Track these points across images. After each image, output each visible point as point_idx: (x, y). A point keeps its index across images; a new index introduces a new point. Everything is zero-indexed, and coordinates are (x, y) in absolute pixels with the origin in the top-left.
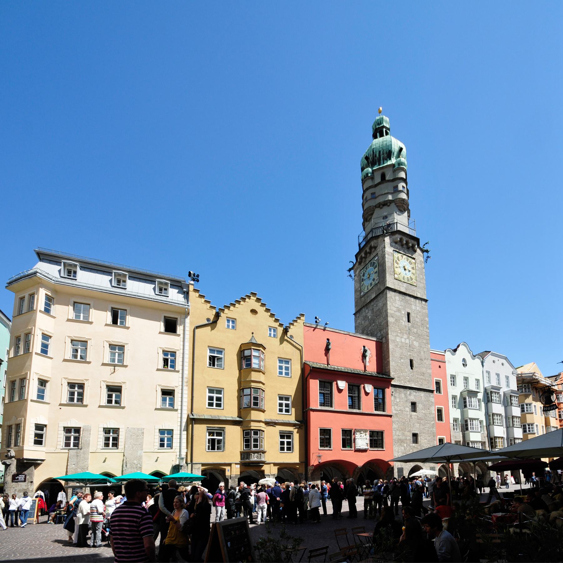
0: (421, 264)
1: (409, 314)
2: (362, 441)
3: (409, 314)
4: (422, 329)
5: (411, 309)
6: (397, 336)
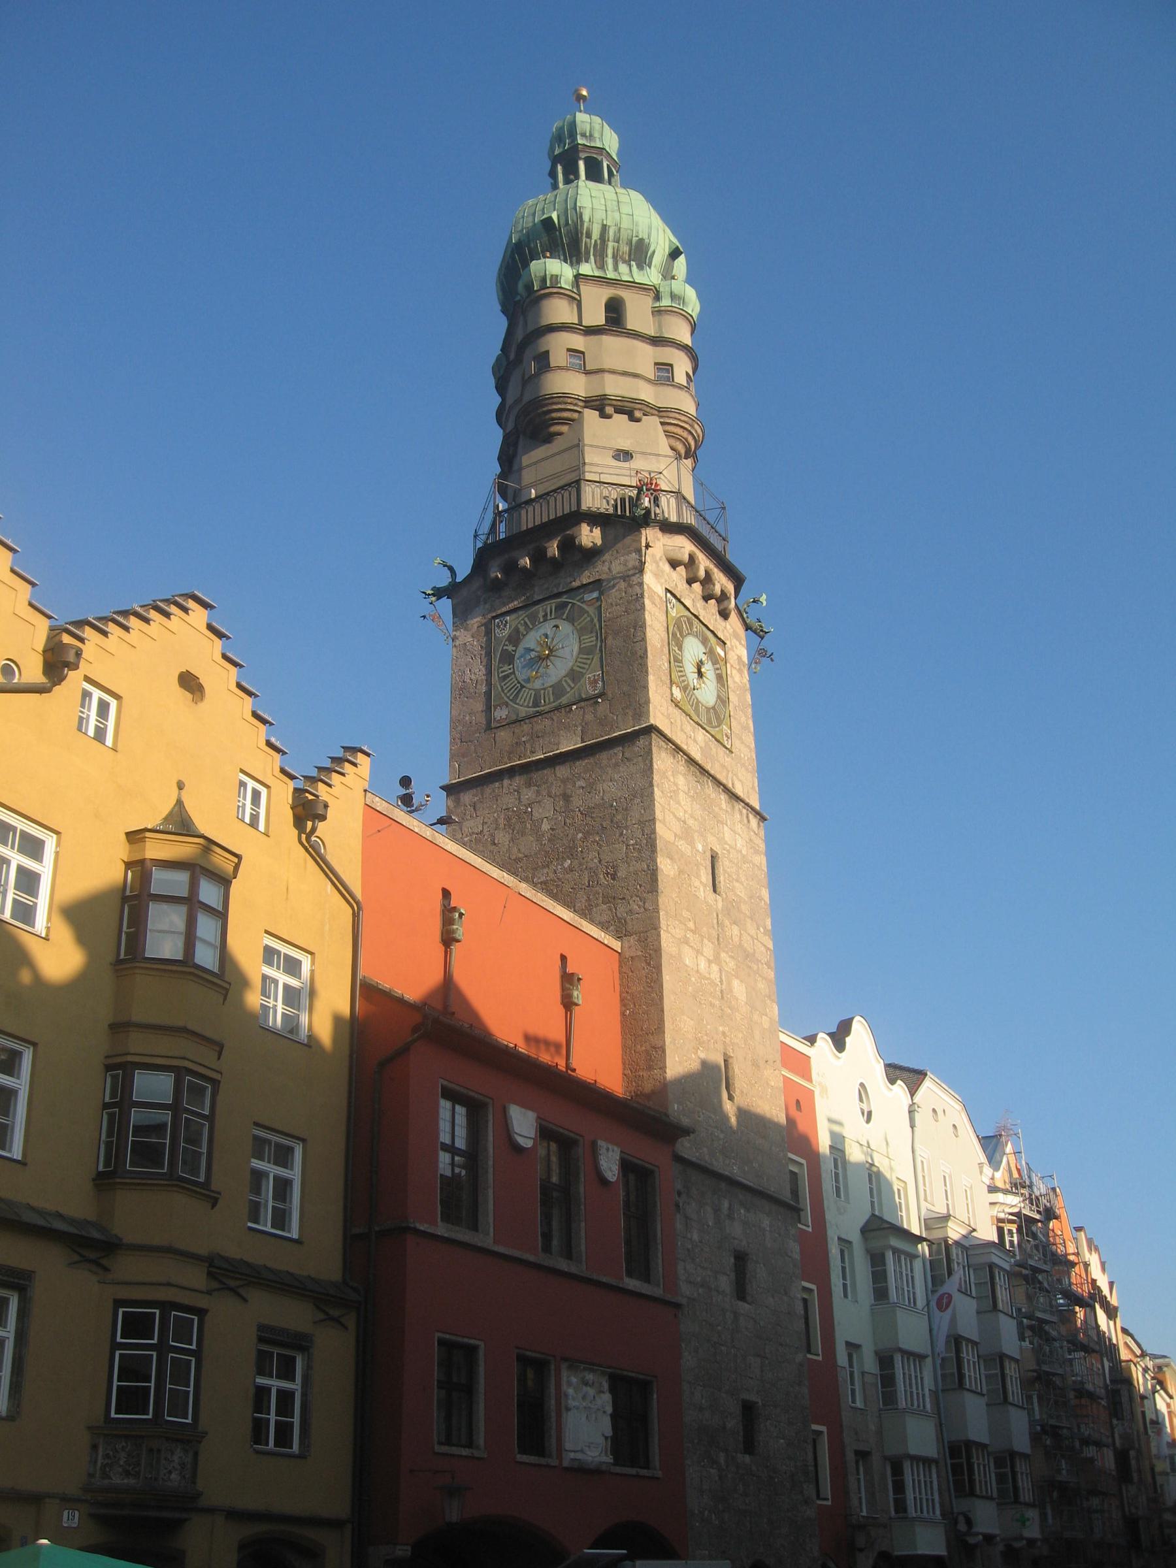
0: (740, 671)
1: (714, 858)
2: (585, 1424)
3: (714, 858)
4: (753, 932)
5: (721, 840)
6: (686, 942)
